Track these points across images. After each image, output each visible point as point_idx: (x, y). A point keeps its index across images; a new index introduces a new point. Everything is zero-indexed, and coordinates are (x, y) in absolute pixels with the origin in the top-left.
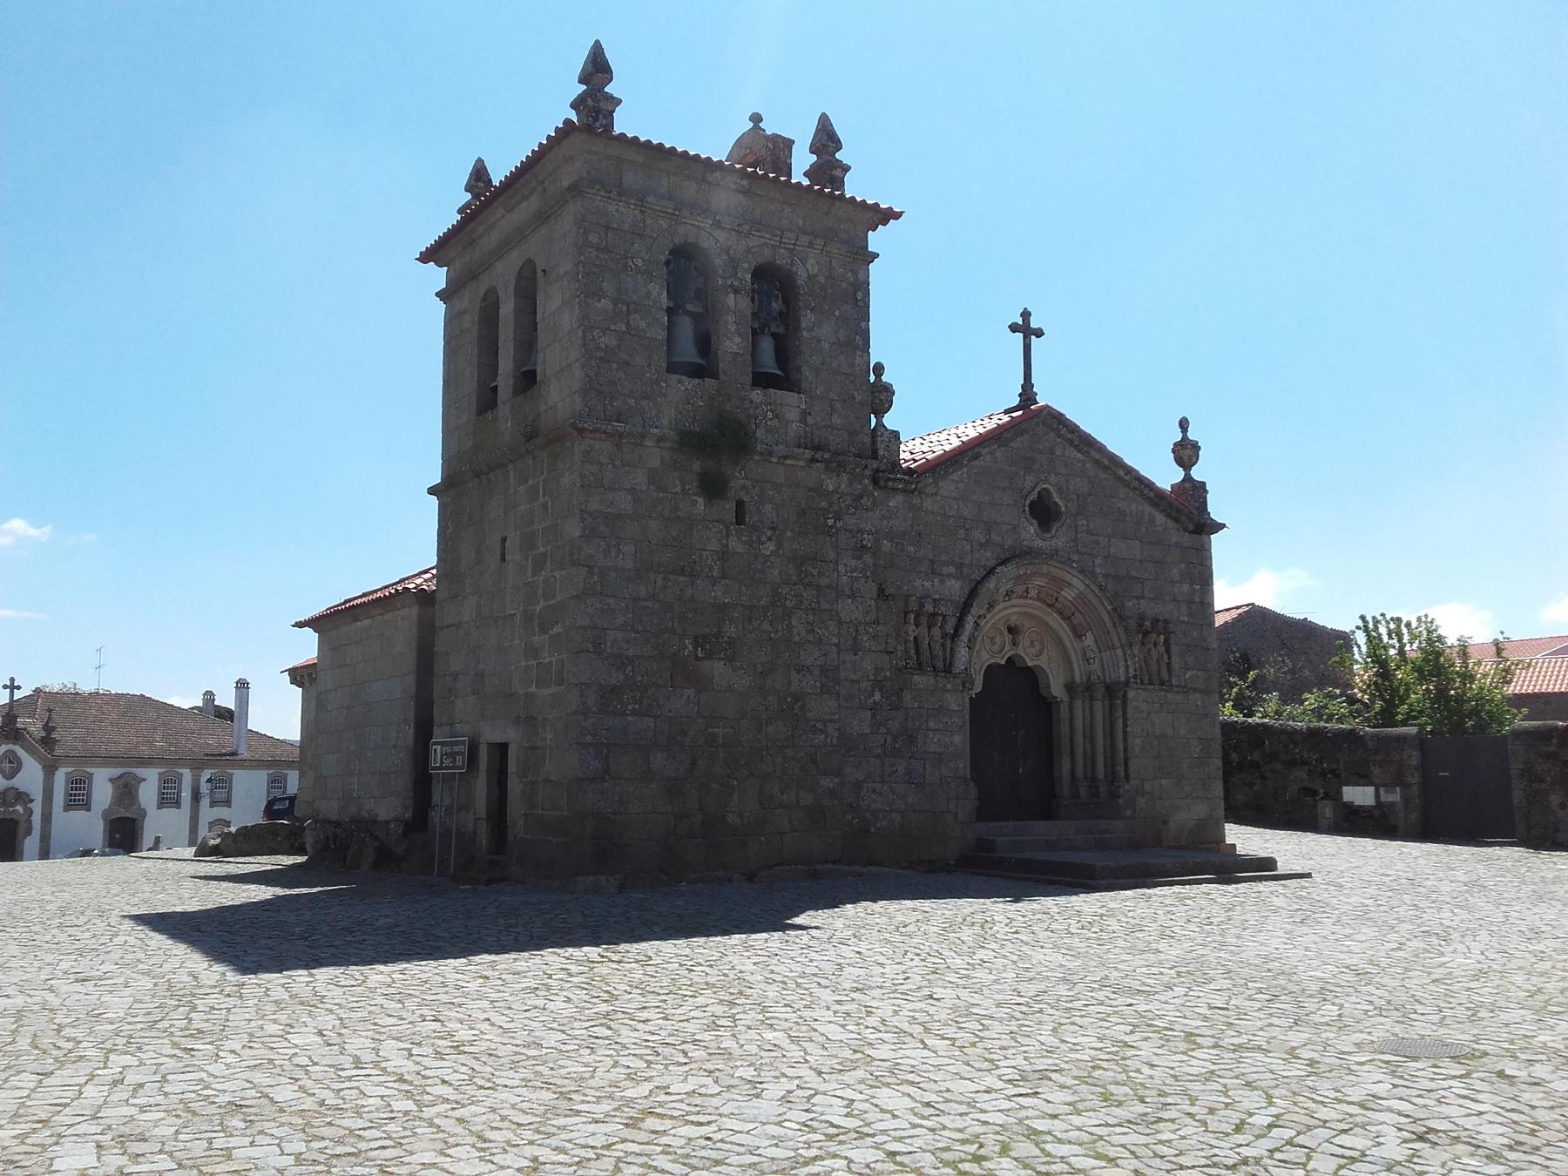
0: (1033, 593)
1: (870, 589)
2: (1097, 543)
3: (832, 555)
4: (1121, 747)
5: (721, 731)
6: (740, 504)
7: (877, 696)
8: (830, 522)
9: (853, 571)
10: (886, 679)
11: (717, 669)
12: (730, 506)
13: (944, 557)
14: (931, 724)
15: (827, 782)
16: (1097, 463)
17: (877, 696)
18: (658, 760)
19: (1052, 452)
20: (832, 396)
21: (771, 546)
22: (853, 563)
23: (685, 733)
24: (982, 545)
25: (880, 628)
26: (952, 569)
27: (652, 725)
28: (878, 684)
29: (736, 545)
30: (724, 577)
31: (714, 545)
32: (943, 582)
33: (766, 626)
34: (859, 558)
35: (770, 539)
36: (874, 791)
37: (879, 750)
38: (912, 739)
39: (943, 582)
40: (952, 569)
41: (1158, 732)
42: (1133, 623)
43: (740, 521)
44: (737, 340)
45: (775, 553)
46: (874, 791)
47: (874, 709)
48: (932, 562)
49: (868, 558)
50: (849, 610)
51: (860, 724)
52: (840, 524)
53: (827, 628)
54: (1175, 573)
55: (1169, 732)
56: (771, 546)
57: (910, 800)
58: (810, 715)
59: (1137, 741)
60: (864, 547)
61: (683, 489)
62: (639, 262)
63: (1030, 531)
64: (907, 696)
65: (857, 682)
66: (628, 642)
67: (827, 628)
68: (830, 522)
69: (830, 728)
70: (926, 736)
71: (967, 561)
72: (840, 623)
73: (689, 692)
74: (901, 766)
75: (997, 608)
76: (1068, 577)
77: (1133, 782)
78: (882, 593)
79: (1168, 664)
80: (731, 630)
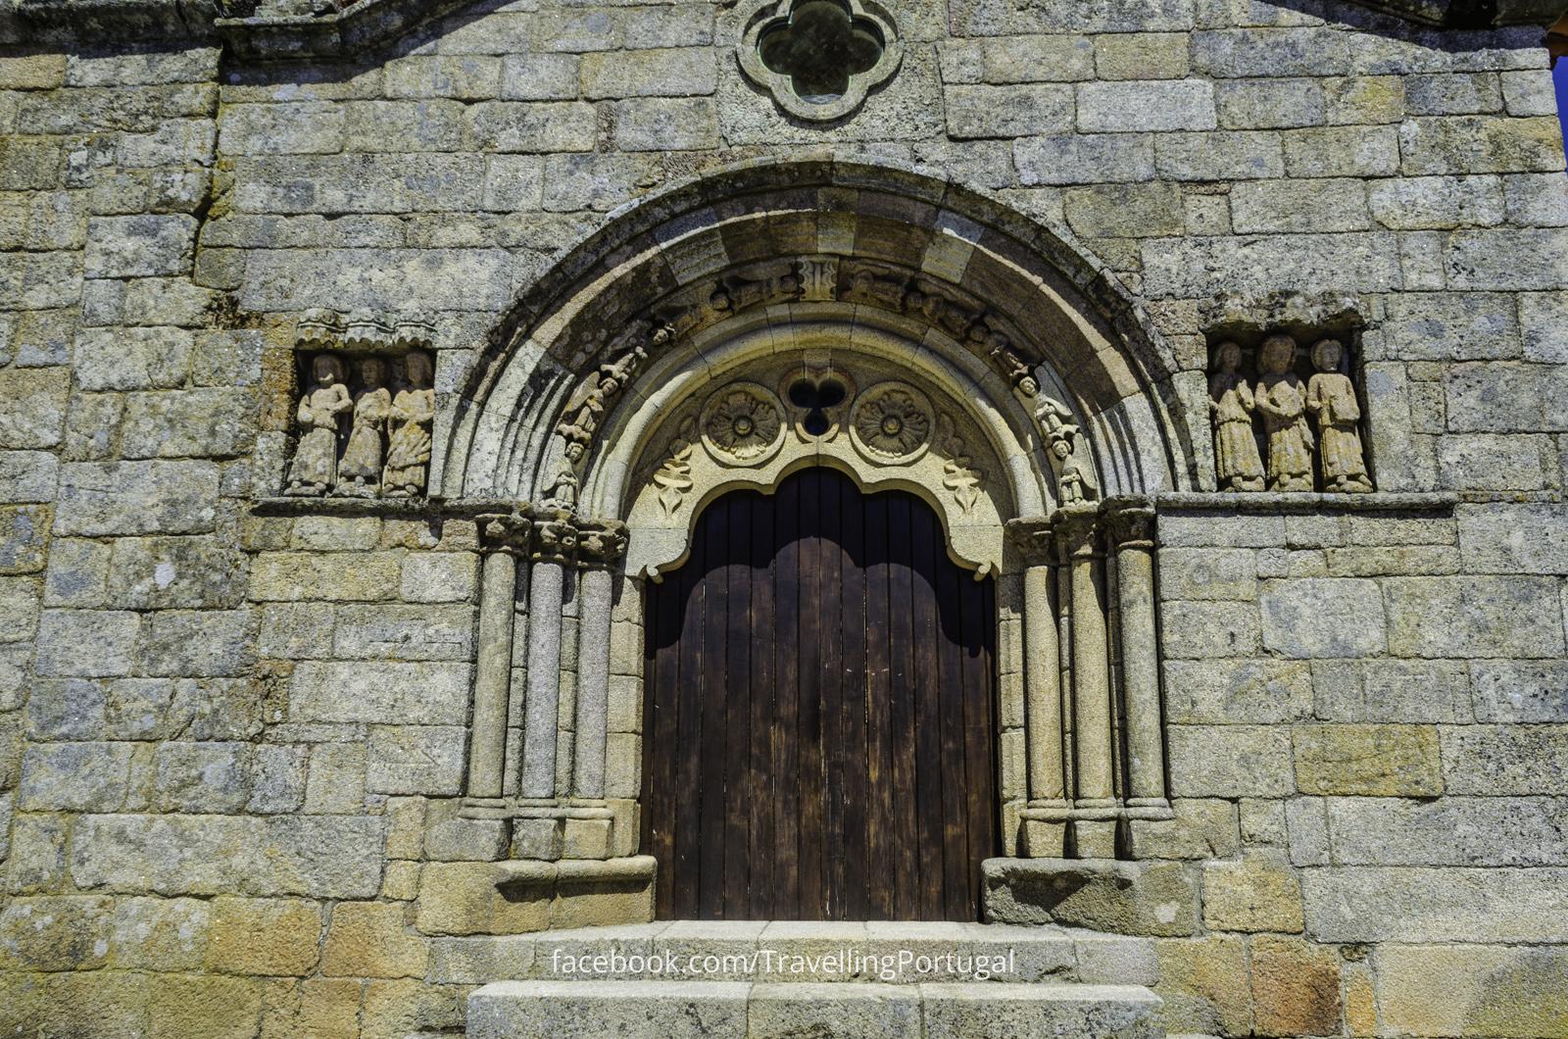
2: (1026, 102)
7: (165, 574)
13: (442, 203)
14: (348, 644)
17: (165, 574)
22: (130, 245)
24: (579, 158)
26: (468, 232)
28: (175, 537)
32: (434, 264)
36: (120, 837)
37: (149, 723)
38: (269, 684)
39: (434, 264)
40: (468, 232)
41: (1310, 643)
46: (120, 837)
50: (104, 359)
59: (1208, 672)
65: (108, 538)
68: (78, 158)
70: (321, 677)
71: (525, 204)
74: (216, 764)
77: (1189, 808)
79: (1361, 425)
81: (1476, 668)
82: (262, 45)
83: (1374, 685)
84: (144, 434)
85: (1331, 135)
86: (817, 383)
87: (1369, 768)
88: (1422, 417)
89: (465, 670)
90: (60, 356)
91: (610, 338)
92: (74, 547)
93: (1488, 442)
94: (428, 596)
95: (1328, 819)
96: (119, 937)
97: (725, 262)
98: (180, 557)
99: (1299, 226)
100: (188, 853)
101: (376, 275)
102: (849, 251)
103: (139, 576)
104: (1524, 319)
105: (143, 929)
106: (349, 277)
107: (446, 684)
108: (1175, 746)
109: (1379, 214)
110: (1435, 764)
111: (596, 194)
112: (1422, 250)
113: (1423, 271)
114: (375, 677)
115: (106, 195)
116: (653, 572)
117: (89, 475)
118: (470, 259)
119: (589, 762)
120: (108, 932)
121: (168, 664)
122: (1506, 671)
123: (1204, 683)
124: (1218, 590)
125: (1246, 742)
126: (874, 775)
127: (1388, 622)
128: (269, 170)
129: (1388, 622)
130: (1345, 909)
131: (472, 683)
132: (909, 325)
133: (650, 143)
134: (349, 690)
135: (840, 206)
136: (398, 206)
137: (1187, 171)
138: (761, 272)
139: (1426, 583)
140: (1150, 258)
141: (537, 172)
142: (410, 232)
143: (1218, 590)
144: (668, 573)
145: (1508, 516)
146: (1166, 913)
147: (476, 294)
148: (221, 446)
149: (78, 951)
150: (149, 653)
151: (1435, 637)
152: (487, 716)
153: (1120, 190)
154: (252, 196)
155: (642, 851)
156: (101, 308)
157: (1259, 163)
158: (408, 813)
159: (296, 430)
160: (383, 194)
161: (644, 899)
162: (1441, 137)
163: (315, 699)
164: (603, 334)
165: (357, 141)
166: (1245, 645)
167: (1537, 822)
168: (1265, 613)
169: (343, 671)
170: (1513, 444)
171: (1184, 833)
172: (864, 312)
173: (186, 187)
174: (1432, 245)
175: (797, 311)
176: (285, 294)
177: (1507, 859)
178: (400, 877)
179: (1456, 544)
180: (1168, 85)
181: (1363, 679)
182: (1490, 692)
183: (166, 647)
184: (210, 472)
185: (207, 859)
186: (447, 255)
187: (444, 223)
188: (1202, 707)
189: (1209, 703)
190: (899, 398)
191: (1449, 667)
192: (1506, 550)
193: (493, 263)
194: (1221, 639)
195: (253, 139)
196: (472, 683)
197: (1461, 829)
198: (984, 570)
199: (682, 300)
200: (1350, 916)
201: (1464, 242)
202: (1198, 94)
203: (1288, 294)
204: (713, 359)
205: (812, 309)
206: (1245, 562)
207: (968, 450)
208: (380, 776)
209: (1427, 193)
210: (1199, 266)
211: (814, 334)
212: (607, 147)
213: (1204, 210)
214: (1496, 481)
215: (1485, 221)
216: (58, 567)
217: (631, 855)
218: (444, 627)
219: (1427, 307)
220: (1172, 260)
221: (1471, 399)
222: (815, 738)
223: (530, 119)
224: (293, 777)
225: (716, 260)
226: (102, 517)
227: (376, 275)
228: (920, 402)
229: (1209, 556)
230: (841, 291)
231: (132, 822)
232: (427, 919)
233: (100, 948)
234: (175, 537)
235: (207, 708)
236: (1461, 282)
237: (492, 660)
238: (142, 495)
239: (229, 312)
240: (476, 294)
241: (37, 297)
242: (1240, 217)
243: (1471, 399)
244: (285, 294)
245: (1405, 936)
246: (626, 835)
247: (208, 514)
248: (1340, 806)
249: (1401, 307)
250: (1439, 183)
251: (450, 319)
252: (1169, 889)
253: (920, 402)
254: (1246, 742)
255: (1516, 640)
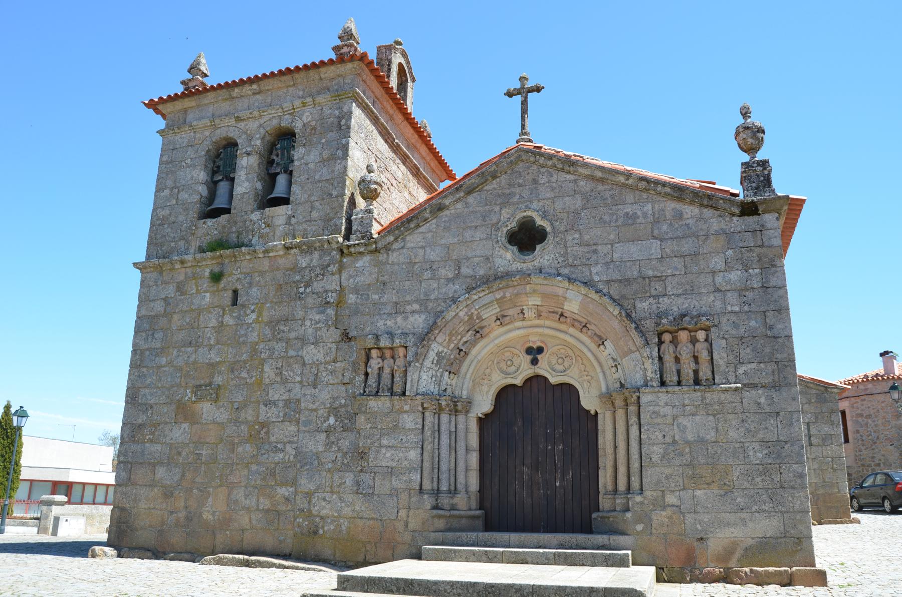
0: (529, 314)
1: (335, 334)
2: (595, 252)
3: (300, 314)
4: (635, 456)
5: (204, 452)
6: (235, 292)
7: (332, 420)
8: (301, 290)
9: (317, 323)
10: (341, 406)
11: (206, 409)
12: (229, 294)
13: (408, 298)
14: (385, 442)
15: (283, 491)
16: (591, 178)
17: (332, 420)
18: (161, 472)
19: (535, 181)
20: (313, 198)
21: (254, 316)
22: (317, 317)
23: (179, 454)
24: (449, 280)
25: (338, 365)
26: (416, 307)
27: (159, 449)
28: (334, 411)
29: (228, 320)
30: (218, 343)
31: (213, 323)
32: (406, 318)
33: (244, 375)
34: (323, 312)
35: (253, 311)
36: (324, 499)
38: (362, 455)
40: (416, 307)
41: (690, 437)
42: (649, 324)
43: (235, 302)
44: (246, 184)
45: (256, 321)
47: (328, 431)
48: (396, 303)
49: (331, 311)
50: (312, 354)
51: (315, 444)
52: (308, 290)
53: (292, 370)
54: (717, 262)
55: (711, 436)
56: (254, 316)
57: (357, 508)
58: (273, 438)
60: (328, 303)
61: (197, 290)
62: (189, 161)
63: (507, 258)
64: (361, 420)
65: (316, 410)
66: (152, 395)
67: (292, 370)
68: (301, 290)
69: (289, 449)
70: (378, 452)
71: (432, 297)
72: (304, 364)
73: (185, 426)
75: (492, 336)
76: (560, 292)
77: (648, 493)
78: (346, 337)
80: (218, 380)
81: (746, 445)
82: (352, 250)
83: (711, 451)
84: (324, 376)
85: (701, 258)
86: (535, 347)
87: (709, 480)
88: (731, 358)
89: (419, 451)
90: (300, 353)
91: (462, 338)
92: (307, 413)
93: (753, 366)
94: (408, 427)
95: (694, 497)
96: (326, 528)
97: (498, 310)
98: (336, 415)
99: (691, 291)
100: (343, 505)
101: (389, 323)
102: (539, 303)
103: (325, 421)
104: (768, 321)
105: (332, 527)
106: (380, 324)
107: (414, 454)
108: (644, 473)
109: (718, 285)
110: (731, 478)
111: (455, 291)
112: (732, 297)
113: (732, 305)
114: (393, 452)
115: (310, 301)
116: (480, 415)
117: (310, 391)
118: (417, 316)
119: (461, 479)
120: (323, 527)
121: (335, 448)
122: (757, 446)
123: (656, 452)
124: (659, 420)
125: (668, 471)
126: (558, 484)
127: (717, 429)
128: (356, 290)
129: (717, 429)
130: (698, 526)
131: (422, 454)
132: (563, 327)
133: (472, 273)
134: (386, 458)
135: (534, 291)
136: (394, 299)
137: (650, 273)
138: (511, 312)
139: (730, 417)
140: (639, 305)
141: (435, 285)
142: (398, 309)
143: (659, 420)
144: (486, 415)
145: (760, 392)
146: (639, 527)
147: (418, 327)
148: (346, 380)
149: (316, 533)
150: (329, 445)
151: (733, 434)
152: (427, 465)
153: (627, 282)
154: (352, 298)
155: (480, 509)
156: (311, 338)
157: (676, 268)
158: (404, 496)
159: (367, 374)
160: (390, 296)
161: (480, 523)
162: (740, 256)
163: (376, 458)
164: (459, 337)
165: (381, 278)
166: (668, 440)
167: (765, 497)
168: (675, 427)
169: (383, 450)
170: (762, 365)
171: (646, 502)
172: (547, 323)
173: (332, 298)
174: (736, 294)
175: (525, 323)
176: (362, 330)
177: (754, 509)
178: (403, 513)
179: (742, 402)
180: (644, 242)
181: (708, 449)
182: (751, 453)
183: (333, 442)
184: (344, 388)
185: (348, 506)
186: (410, 315)
187: (409, 304)
188: (653, 460)
189: (655, 458)
190: (563, 351)
191: (737, 445)
192: (759, 404)
193: (423, 317)
194: (660, 437)
195: (351, 280)
196: (422, 454)
197: (739, 499)
198: (593, 412)
199: (484, 323)
200: (700, 528)
201: (747, 294)
202: (654, 245)
203: (685, 316)
204: (496, 342)
205: (529, 323)
206: (668, 410)
207: (587, 369)
208: (395, 483)
209: (735, 276)
210: (654, 307)
211: (530, 330)
212: (458, 276)
213: (658, 287)
214: (757, 381)
215: (755, 286)
216: (303, 418)
217: (476, 510)
218: (412, 437)
219: (733, 318)
220: (645, 305)
221: (748, 350)
222: (538, 471)
223: (434, 267)
224: (371, 482)
225: (495, 310)
226: (314, 402)
227: (389, 323)
228: (570, 353)
229: (657, 408)
230: (539, 316)
231: (327, 496)
232: (411, 526)
233: (321, 532)
234: (334, 411)
235: (346, 461)
236: (746, 308)
237: (428, 447)
238: (325, 395)
239: (346, 337)
240: (418, 327)
241: (293, 335)
242: (669, 289)
243: (748, 350)
244: (362, 330)
245: (719, 535)
246: (474, 504)
247: (343, 401)
248: (698, 493)
249: (724, 320)
250: (739, 272)
251: (411, 336)
252: (639, 521)
253: (570, 353)
254: (668, 471)
255: (761, 435)
